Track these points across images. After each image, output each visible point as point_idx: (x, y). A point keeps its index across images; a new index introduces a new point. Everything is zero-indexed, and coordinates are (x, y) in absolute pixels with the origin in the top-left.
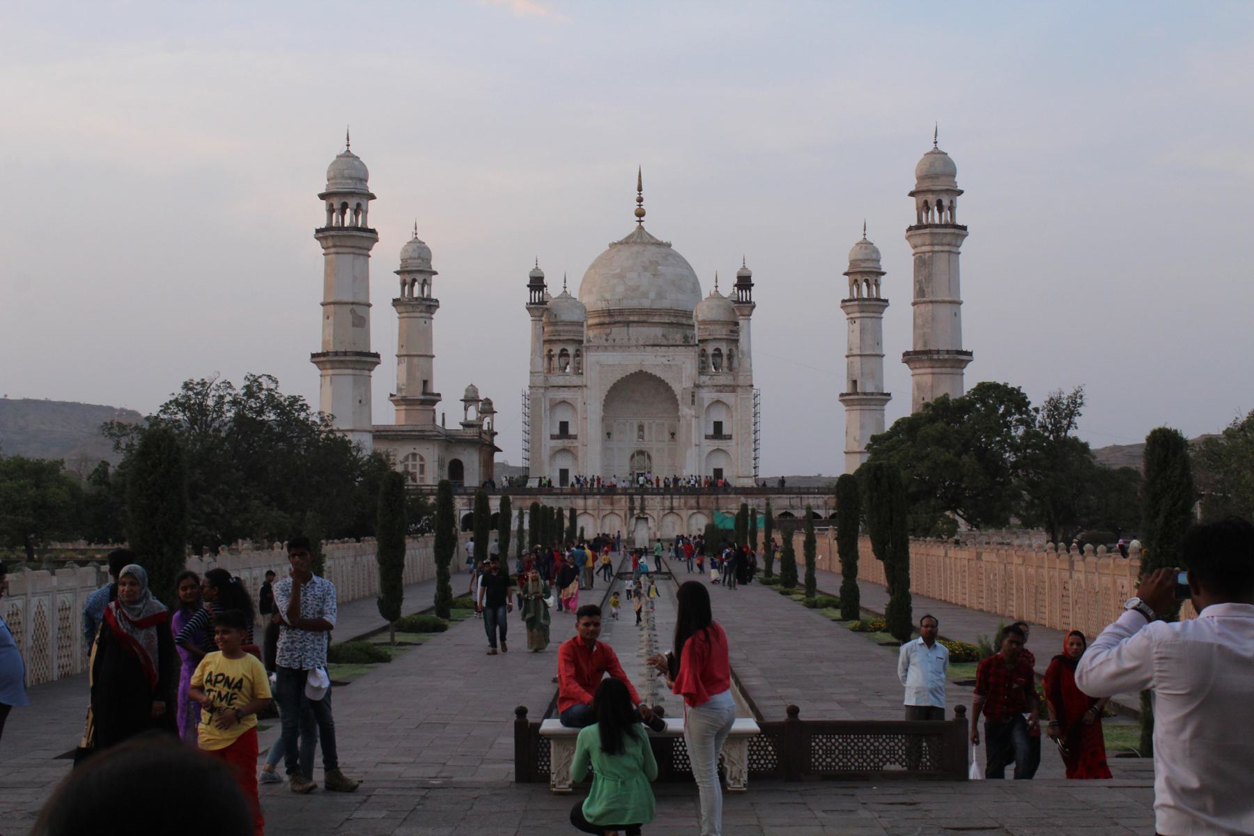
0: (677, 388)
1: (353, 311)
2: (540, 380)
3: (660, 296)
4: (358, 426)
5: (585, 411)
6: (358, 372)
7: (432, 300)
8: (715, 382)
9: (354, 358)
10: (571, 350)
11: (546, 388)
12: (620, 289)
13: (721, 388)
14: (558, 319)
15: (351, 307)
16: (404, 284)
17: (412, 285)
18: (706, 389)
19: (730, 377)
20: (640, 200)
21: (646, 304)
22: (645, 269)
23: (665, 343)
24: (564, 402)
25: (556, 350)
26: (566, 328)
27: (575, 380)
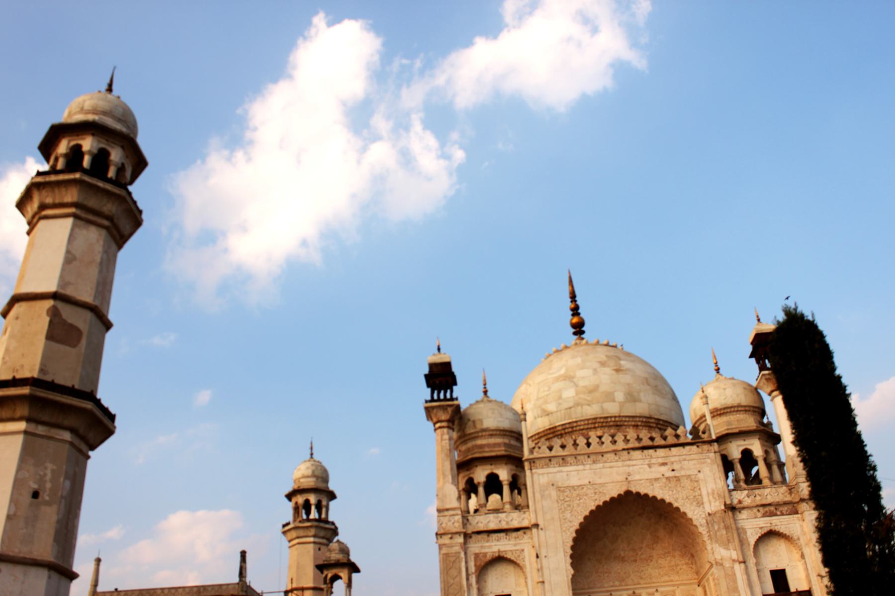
0: (696, 514)
1: (54, 313)
2: (455, 523)
3: (632, 397)
4: (18, 550)
5: (540, 570)
6: (41, 430)
7: (326, 521)
8: (758, 500)
9: (25, 390)
10: (504, 474)
11: (467, 536)
12: (569, 393)
13: (770, 509)
14: (479, 427)
15: (50, 303)
16: (296, 509)
17: (308, 513)
18: (744, 515)
19: (784, 489)
20: (575, 311)
21: (612, 409)
22: (603, 364)
23: (663, 442)
24: (499, 559)
25: (480, 475)
26: (492, 441)
27: (516, 519)
